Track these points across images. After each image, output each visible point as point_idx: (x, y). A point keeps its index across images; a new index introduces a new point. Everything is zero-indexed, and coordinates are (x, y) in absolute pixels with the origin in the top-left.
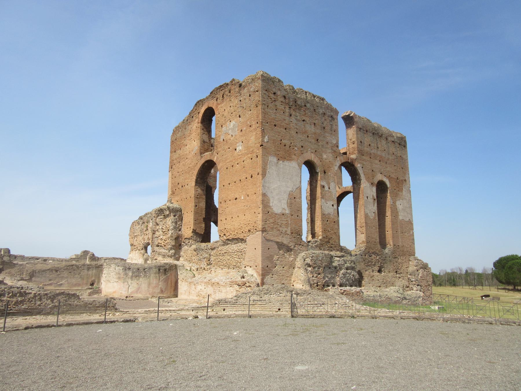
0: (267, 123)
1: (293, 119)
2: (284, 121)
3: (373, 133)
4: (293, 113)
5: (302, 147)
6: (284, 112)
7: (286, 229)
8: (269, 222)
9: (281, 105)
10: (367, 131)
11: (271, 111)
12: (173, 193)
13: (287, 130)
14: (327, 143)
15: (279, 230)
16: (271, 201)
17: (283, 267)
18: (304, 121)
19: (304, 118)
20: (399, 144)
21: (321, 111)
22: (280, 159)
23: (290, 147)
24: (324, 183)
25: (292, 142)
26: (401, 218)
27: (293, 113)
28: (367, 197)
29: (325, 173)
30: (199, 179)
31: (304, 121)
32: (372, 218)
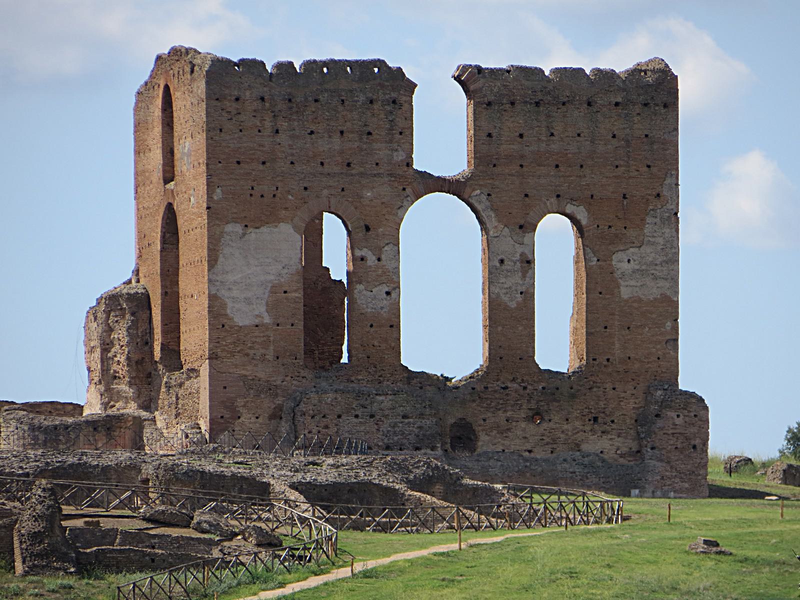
0: (220, 162)
1: (282, 138)
2: (261, 148)
3: (537, 104)
4: (283, 125)
5: (306, 189)
6: (259, 131)
7: (263, 351)
8: (224, 343)
9: (253, 119)
10: (513, 104)
11: (228, 137)
12: (140, 257)
13: (268, 164)
14: (377, 164)
15: (247, 355)
16: (230, 305)
17: (257, 418)
18: (312, 133)
19: (313, 128)
20: (646, 105)
21: (362, 98)
22: (249, 226)
23: (274, 196)
24: (365, 252)
25: (279, 184)
26: (625, 293)
27: (283, 125)
28: (502, 261)
29: (368, 229)
30: (168, 235)
31: (312, 133)
32: (513, 305)
